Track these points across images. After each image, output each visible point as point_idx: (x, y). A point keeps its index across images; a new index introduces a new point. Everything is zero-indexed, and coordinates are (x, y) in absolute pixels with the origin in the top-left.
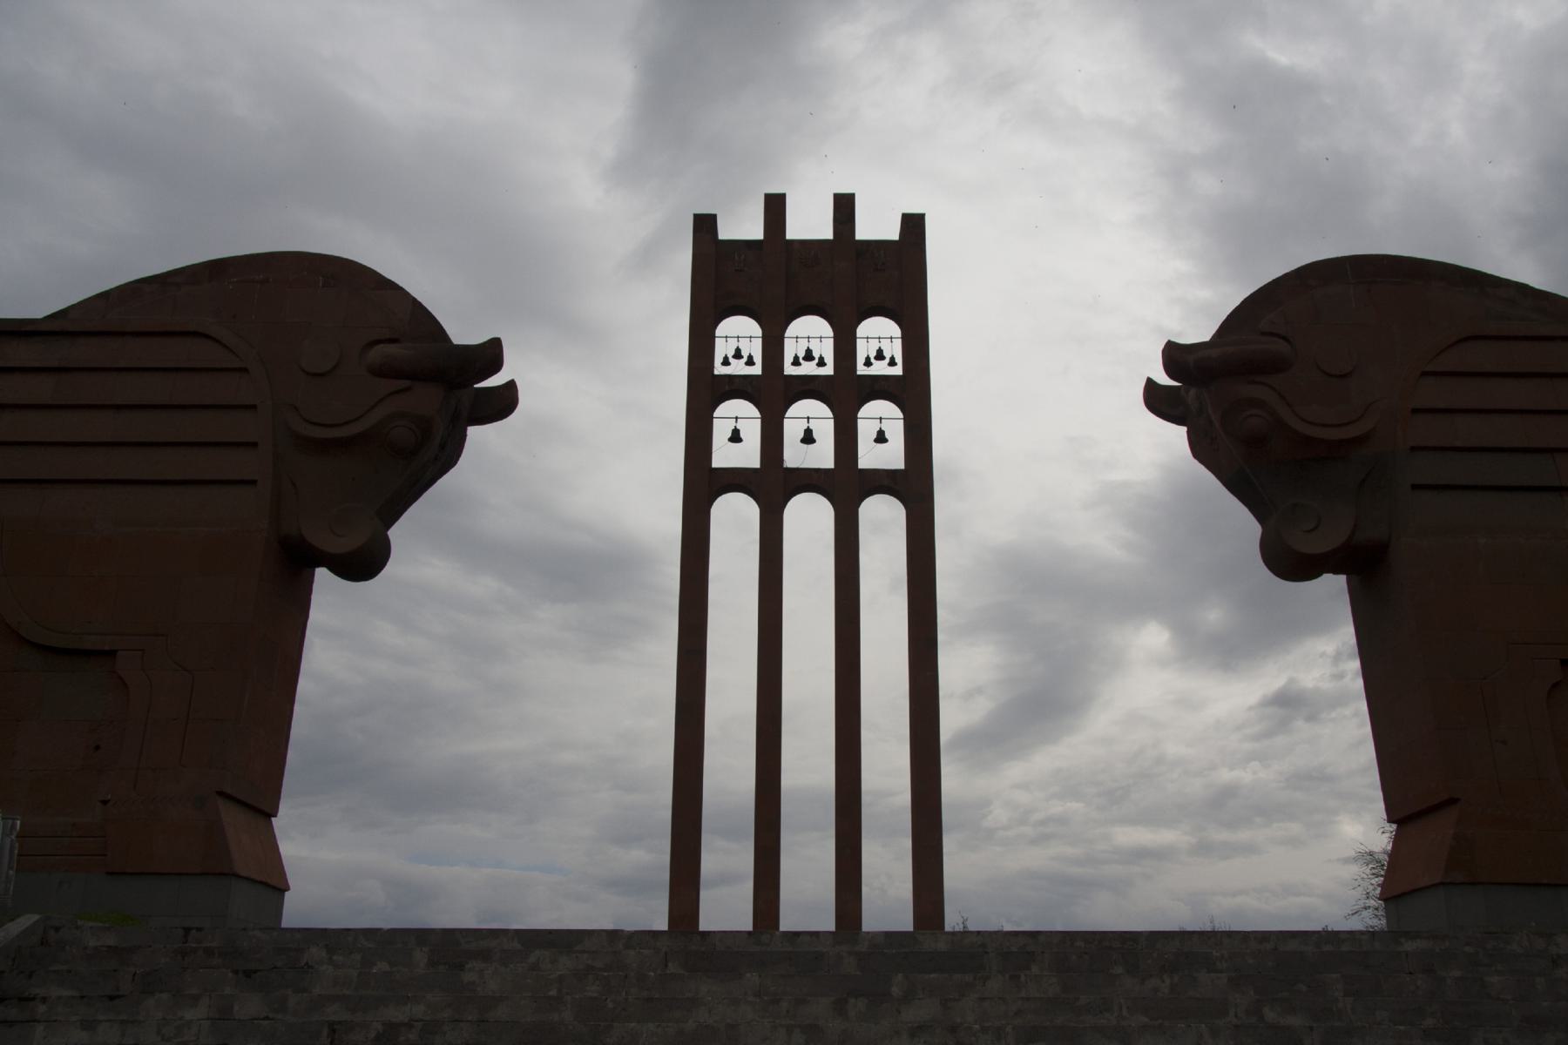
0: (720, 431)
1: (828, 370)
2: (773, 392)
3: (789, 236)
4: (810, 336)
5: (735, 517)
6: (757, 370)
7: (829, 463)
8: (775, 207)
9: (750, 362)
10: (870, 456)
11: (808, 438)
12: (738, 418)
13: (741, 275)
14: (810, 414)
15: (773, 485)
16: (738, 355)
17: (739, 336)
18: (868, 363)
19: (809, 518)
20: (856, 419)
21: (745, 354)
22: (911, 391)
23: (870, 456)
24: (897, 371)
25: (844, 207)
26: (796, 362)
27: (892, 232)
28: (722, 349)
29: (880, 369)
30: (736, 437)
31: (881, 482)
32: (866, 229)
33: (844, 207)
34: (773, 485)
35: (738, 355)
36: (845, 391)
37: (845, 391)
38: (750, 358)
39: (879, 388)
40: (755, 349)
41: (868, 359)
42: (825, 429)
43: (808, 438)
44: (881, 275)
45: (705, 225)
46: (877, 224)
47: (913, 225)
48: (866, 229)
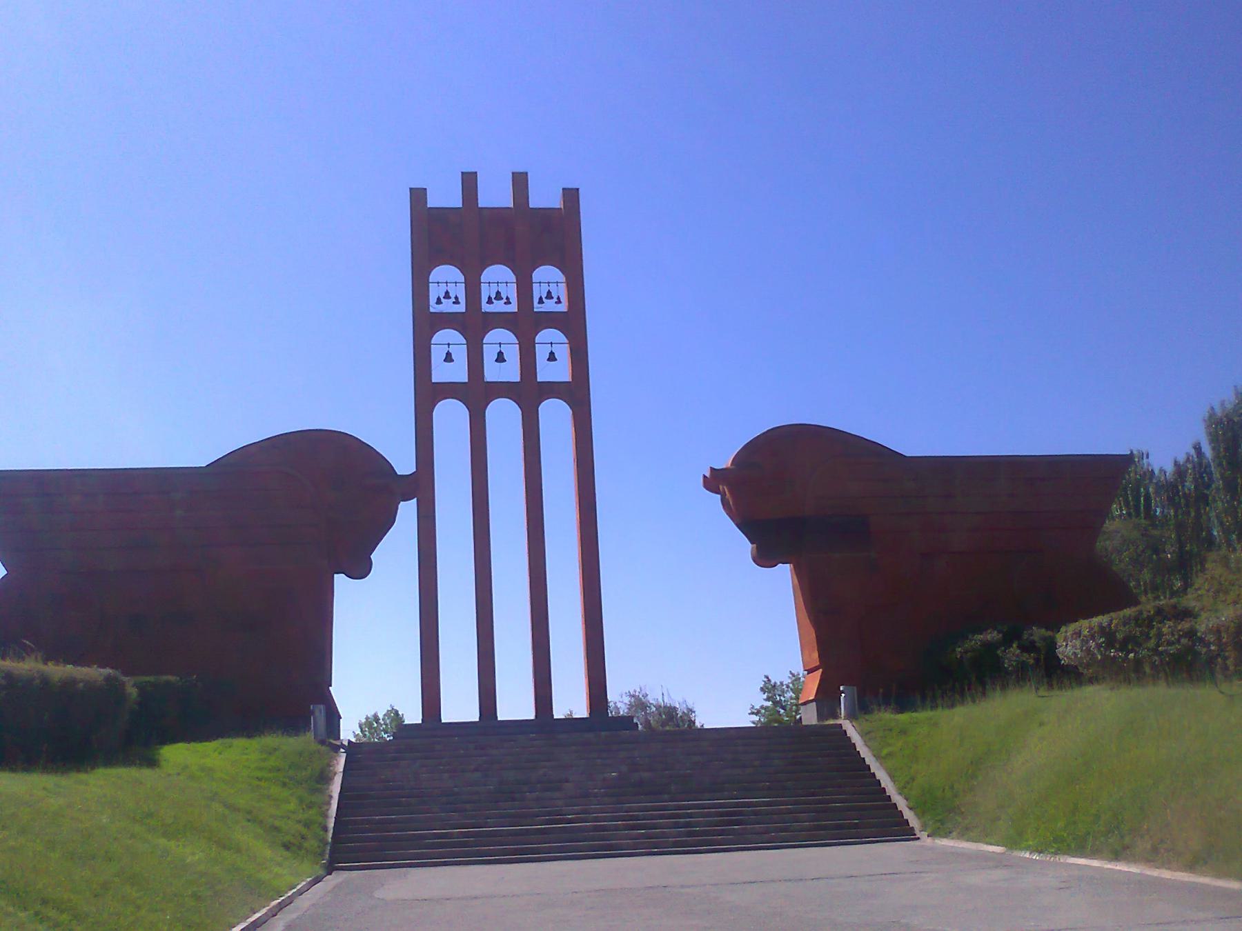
0: (437, 354)
1: (513, 308)
2: (474, 325)
3: (482, 203)
5: (451, 418)
6: (461, 308)
7: (516, 378)
8: (469, 182)
9: (457, 302)
11: (500, 358)
12: (448, 340)
13: (448, 234)
14: (499, 339)
15: (477, 394)
16: (447, 296)
18: (541, 301)
19: (503, 416)
20: (534, 344)
21: (452, 295)
22: (573, 323)
23: (548, 372)
24: (563, 307)
25: (520, 182)
26: (490, 301)
27: (556, 202)
28: (435, 292)
29: (550, 306)
30: (449, 358)
31: (552, 390)
32: (535, 201)
33: (520, 182)
34: (477, 394)
35: (447, 296)
36: (525, 324)
37: (525, 324)
38: (456, 298)
39: (551, 320)
40: (460, 291)
41: (541, 298)
42: (513, 353)
43: (500, 358)
45: (418, 196)
46: (544, 196)
47: (571, 196)
48: (535, 201)
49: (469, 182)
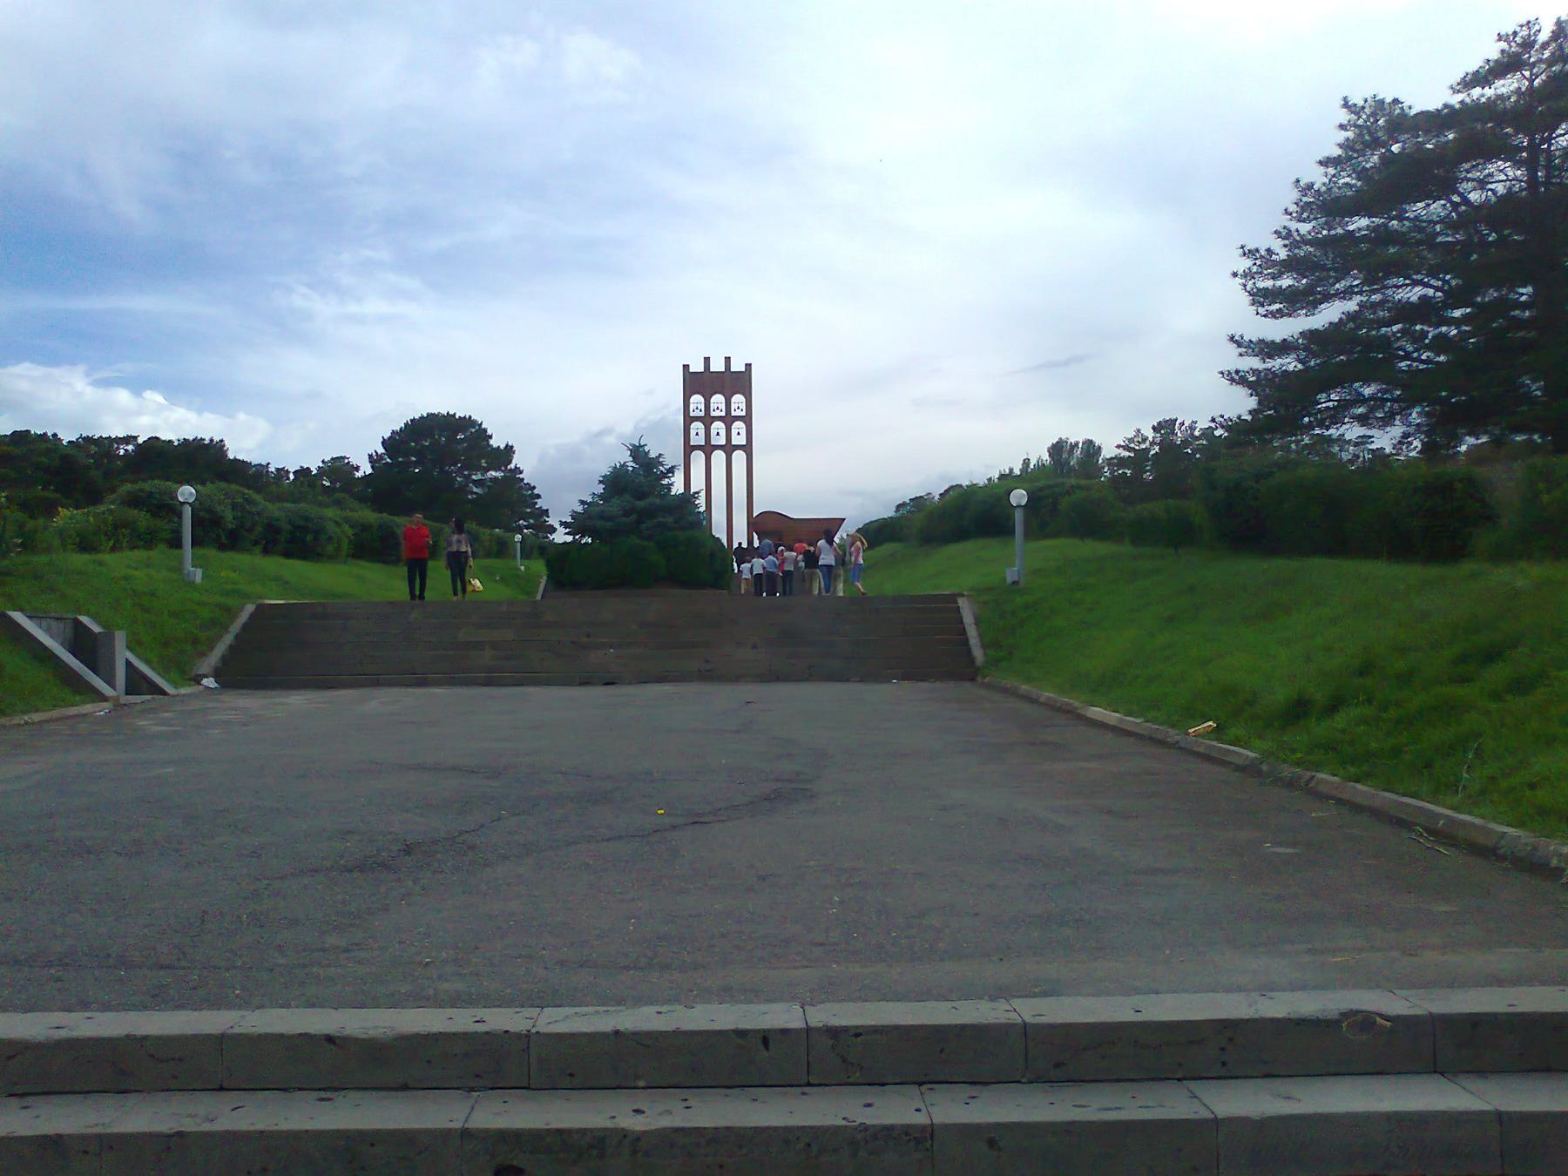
0: (693, 433)
2: (707, 420)
4: (718, 400)
5: (698, 459)
8: (707, 360)
10: (736, 440)
12: (697, 426)
13: (698, 382)
14: (718, 426)
15: (708, 449)
17: (697, 400)
19: (719, 457)
22: (747, 420)
23: (736, 440)
25: (728, 359)
28: (692, 407)
29: (739, 413)
33: (728, 359)
34: (708, 449)
36: (728, 420)
37: (728, 420)
42: (723, 433)
44: (736, 382)
45: (686, 367)
46: (737, 366)
47: (748, 366)
49: (707, 360)
